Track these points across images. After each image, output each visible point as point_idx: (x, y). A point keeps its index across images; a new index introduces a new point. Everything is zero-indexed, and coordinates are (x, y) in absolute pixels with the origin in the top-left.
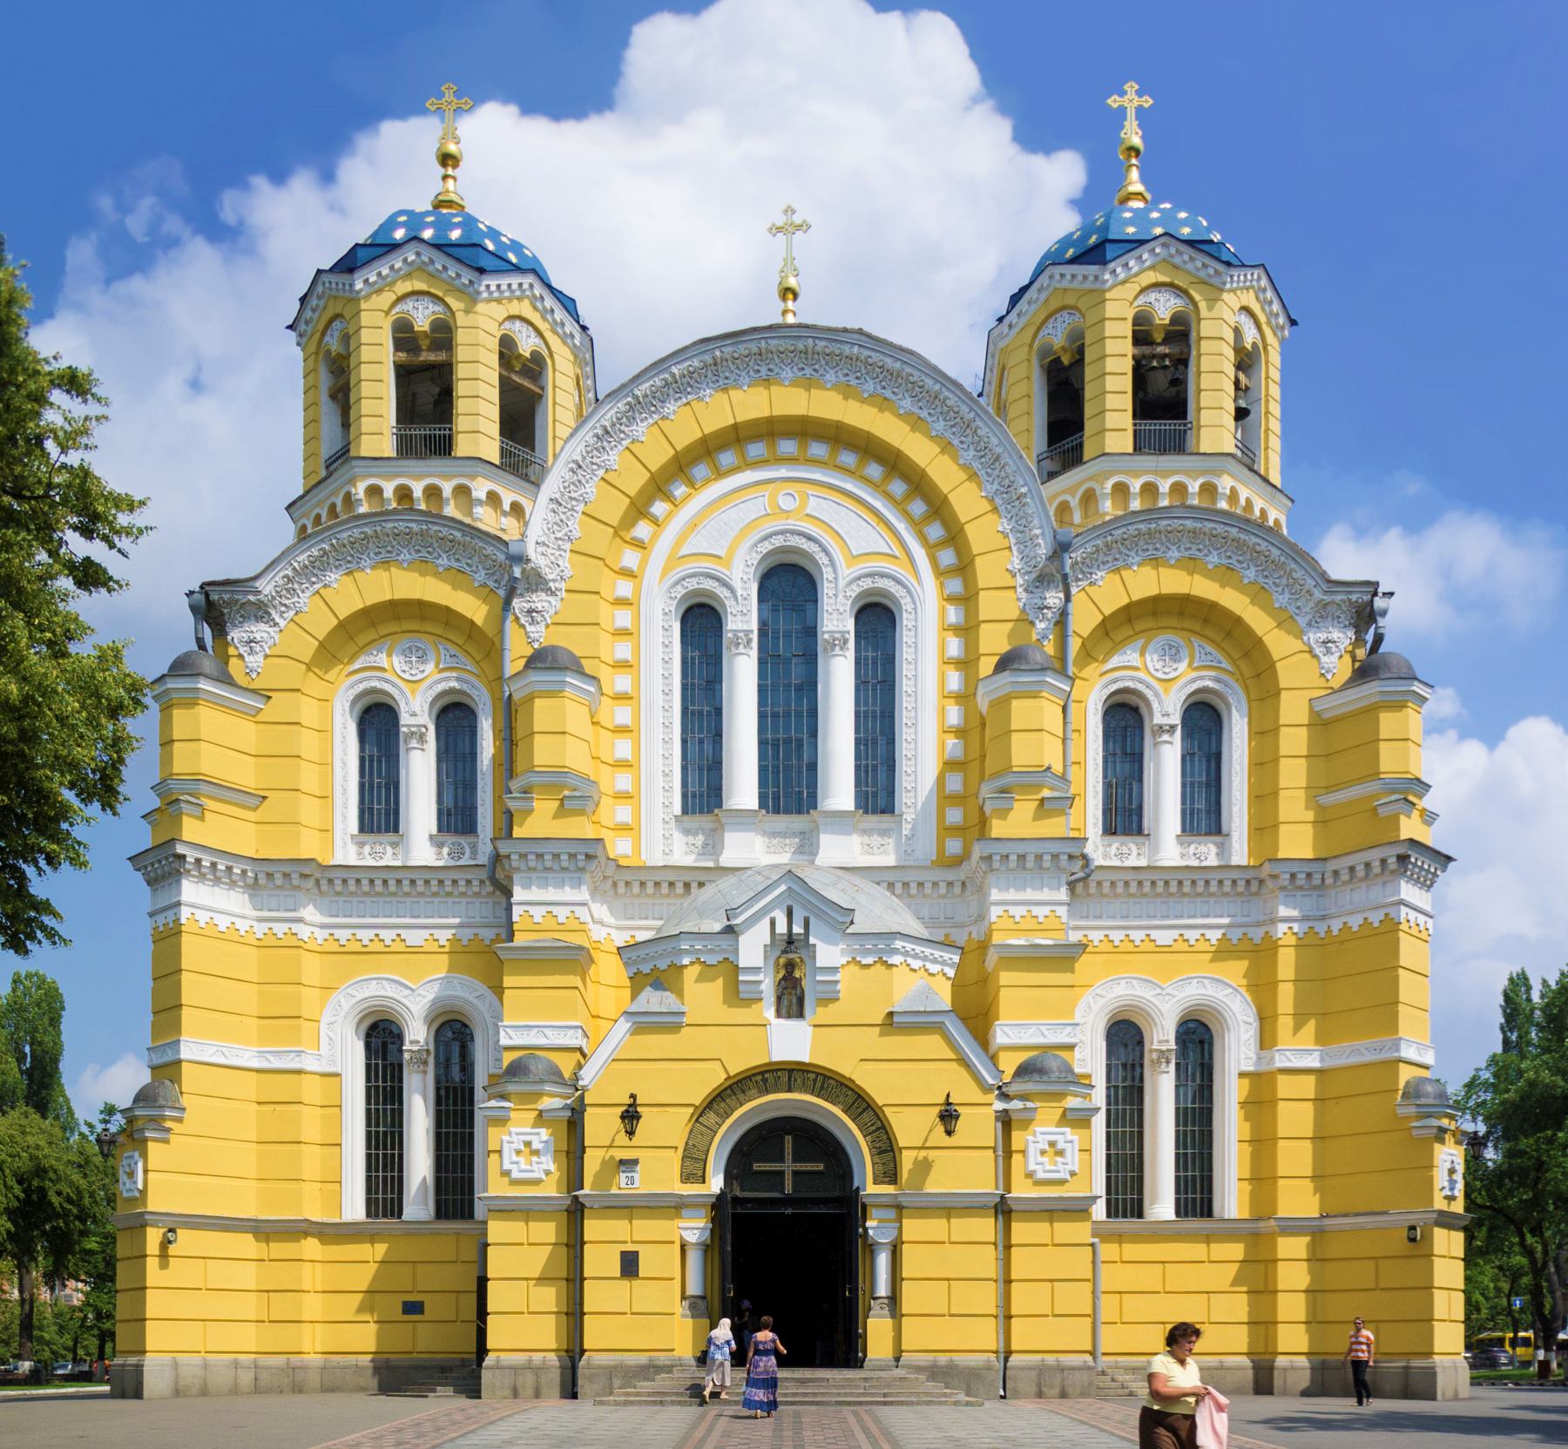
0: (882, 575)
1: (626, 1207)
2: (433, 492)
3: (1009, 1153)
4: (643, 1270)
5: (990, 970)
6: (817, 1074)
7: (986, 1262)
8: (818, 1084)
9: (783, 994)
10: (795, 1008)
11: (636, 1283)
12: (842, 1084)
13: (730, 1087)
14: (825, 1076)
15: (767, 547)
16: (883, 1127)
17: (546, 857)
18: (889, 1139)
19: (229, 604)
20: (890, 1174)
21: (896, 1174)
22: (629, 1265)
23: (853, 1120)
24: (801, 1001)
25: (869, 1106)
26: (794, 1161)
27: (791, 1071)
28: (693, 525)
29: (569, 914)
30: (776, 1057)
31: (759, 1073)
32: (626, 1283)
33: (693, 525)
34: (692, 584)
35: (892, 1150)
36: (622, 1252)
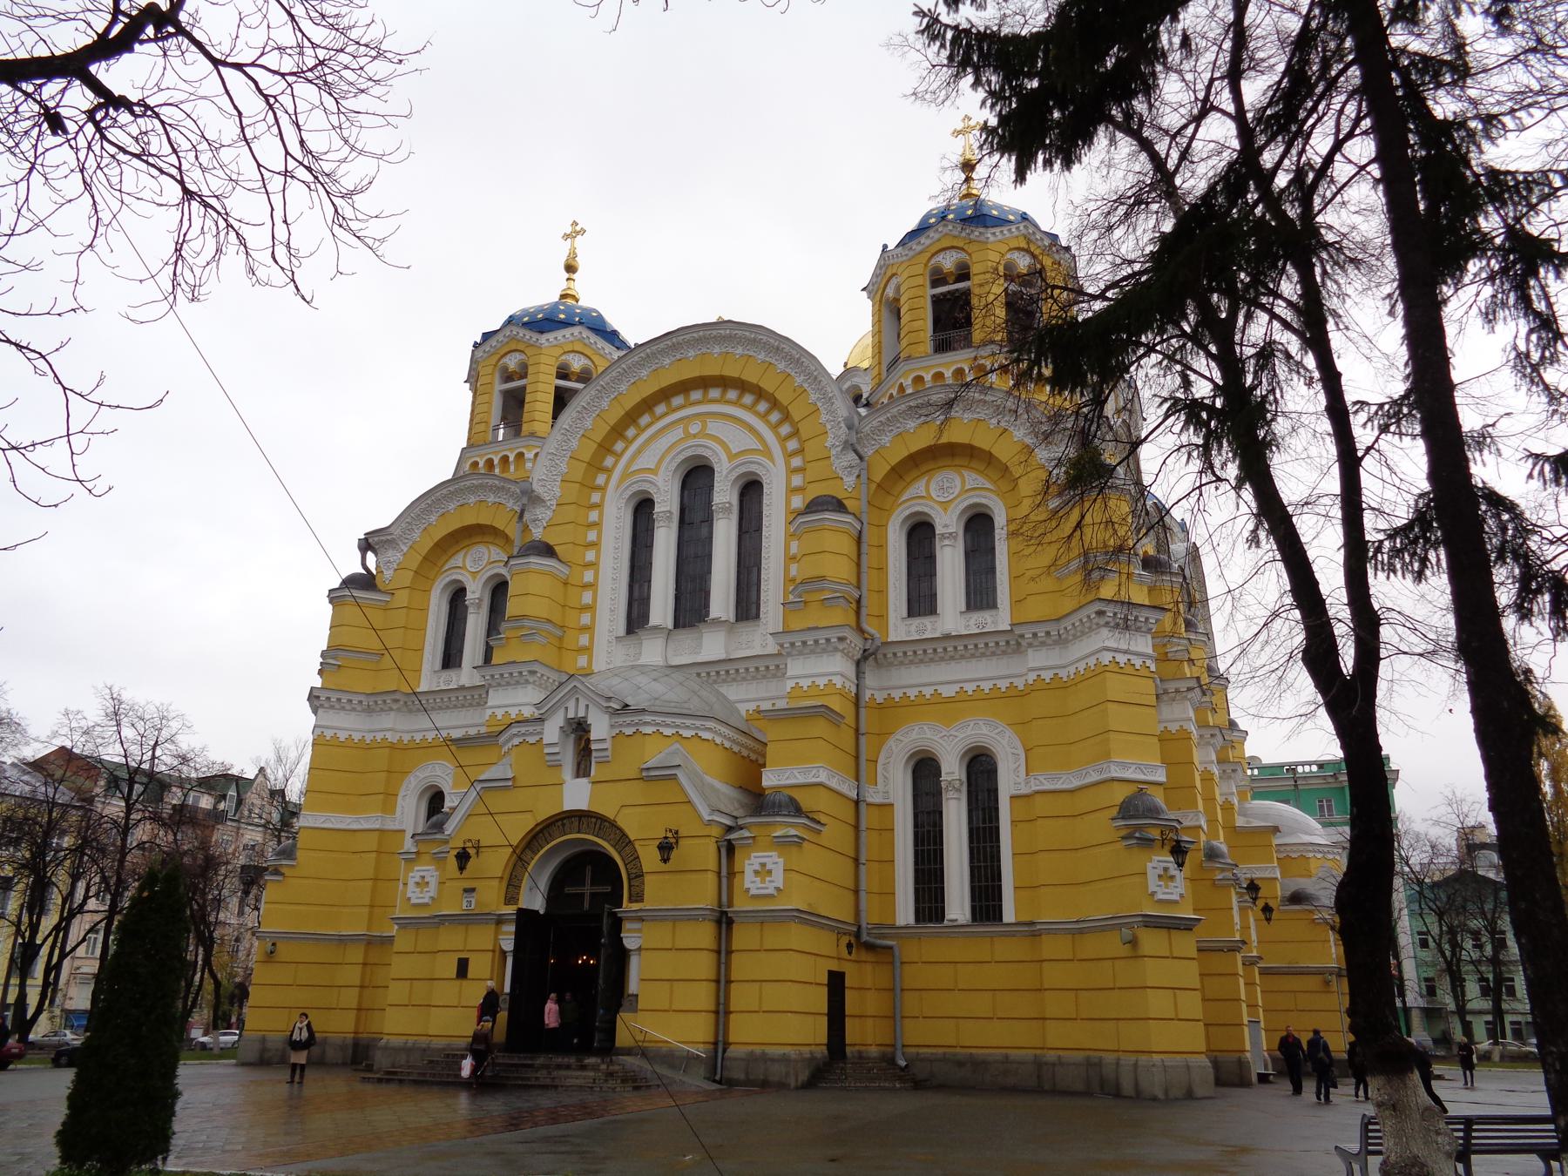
0: (751, 462)
2: (505, 459)
3: (731, 874)
4: (471, 973)
7: (704, 965)
11: (464, 982)
13: (541, 831)
15: (682, 457)
19: (377, 543)
20: (637, 897)
22: (463, 968)
23: (619, 853)
26: (592, 885)
27: (580, 817)
28: (639, 451)
30: (567, 807)
32: (458, 982)
33: (639, 451)
34: (636, 488)
36: (460, 960)
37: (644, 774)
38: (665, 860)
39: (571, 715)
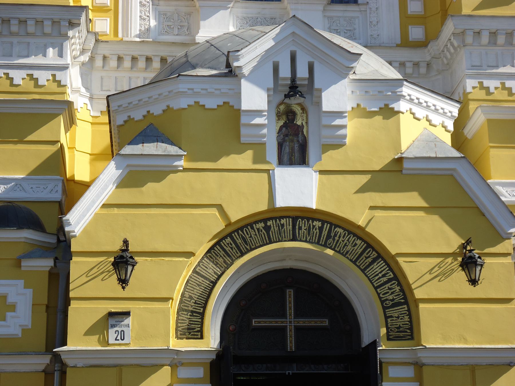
1: (115, 366)
5: (469, 137)
6: (323, 222)
8: (325, 233)
9: (284, 141)
10: (297, 155)
12: (350, 233)
13: (230, 235)
14: (331, 224)
16: (395, 278)
17: (29, 22)
18: (402, 290)
21: (411, 329)
24: (303, 148)
25: (379, 256)
26: (297, 316)
27: (295, 219)
29: (51, 78)
31: (260, 221)
35: (406, 303)
37: (406, 165)
38: (474, 282)
39: (285, 72)
